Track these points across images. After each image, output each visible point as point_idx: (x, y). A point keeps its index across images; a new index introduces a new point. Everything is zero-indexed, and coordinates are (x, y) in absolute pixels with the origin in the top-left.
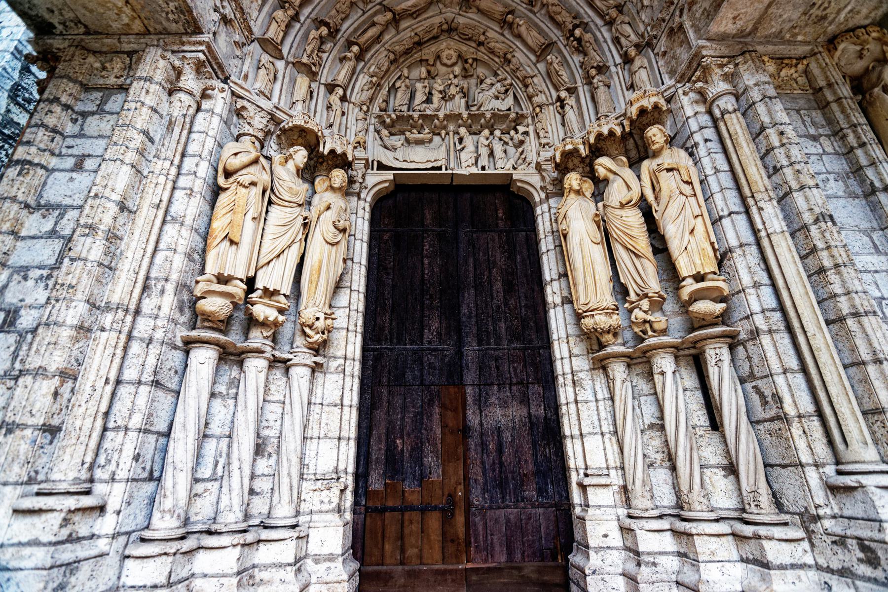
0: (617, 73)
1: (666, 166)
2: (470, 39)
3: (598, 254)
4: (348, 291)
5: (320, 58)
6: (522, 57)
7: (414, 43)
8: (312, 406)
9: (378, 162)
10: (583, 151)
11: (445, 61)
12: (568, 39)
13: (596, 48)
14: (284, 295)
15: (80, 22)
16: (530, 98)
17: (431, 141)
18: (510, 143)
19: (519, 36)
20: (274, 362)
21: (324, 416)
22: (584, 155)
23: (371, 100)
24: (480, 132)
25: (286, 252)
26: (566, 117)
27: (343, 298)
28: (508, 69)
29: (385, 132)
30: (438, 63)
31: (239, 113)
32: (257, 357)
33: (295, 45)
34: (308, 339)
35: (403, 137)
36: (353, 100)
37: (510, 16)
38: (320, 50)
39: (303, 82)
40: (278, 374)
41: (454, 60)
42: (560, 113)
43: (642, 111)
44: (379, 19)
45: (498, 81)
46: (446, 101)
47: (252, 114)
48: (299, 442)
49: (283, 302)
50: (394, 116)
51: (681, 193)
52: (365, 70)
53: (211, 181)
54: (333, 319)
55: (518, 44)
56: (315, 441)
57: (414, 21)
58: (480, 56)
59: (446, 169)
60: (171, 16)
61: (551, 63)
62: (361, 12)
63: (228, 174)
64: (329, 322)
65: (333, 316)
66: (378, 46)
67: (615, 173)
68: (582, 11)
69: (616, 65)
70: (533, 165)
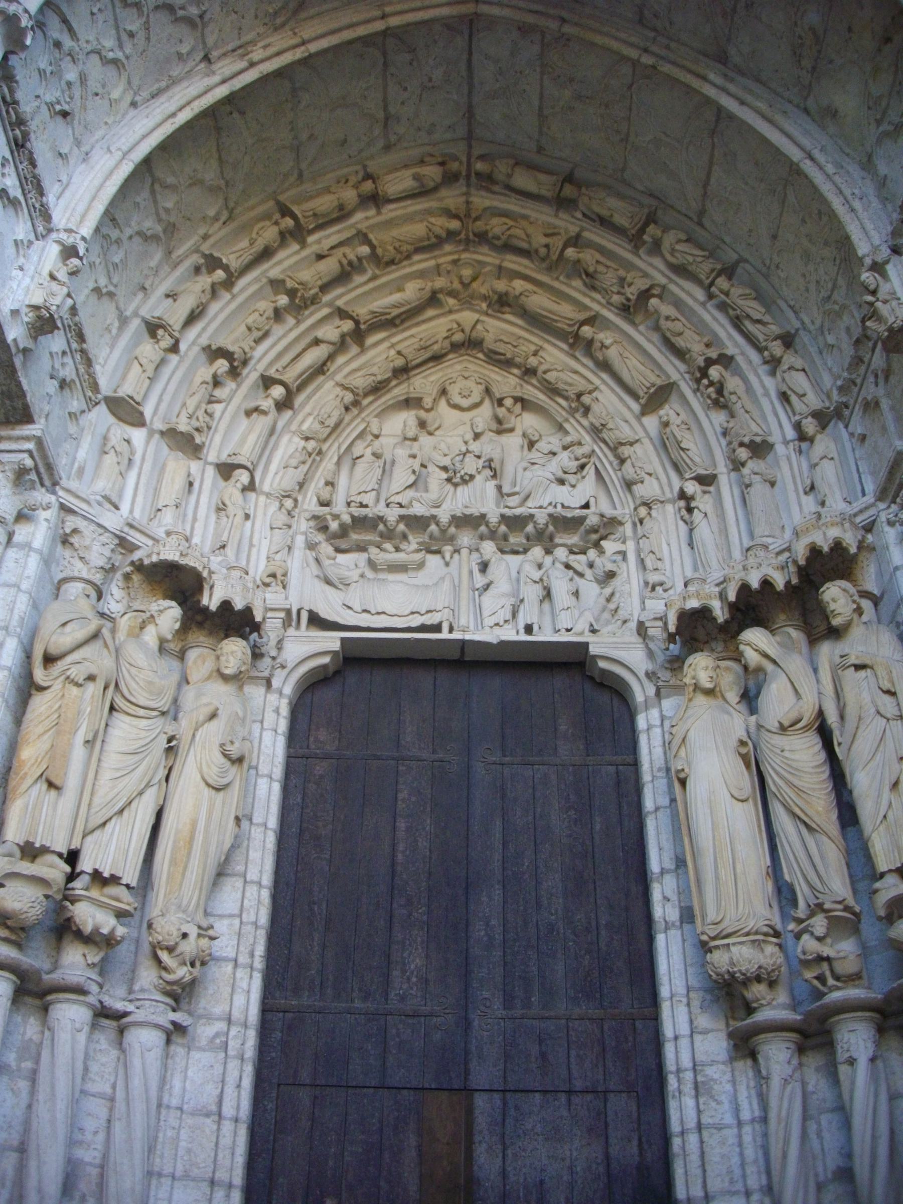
0: (789, 459)
1: (853, 660)
3: (743, 820)
4: (239, 883)
5: (211, 415)
6: (609, 402)
8: (164, 1112)
10: (720, 613)
11: (457, 400)
12: (698, 381)
14: (128, 886)
16: (629, 485)
17: (421, 565)
19: (605, 366)
20: (103, 1013)
21: (184, 1134)
22: (721, 620)
23: (301, 485)
24: (525, 551)
25: (134, 804)
27: (229, 897)
28: (585, 423)
29: (326, 549)
30: (443, 403)
31: (65, 541)
32: (75, 1002)
34: (164, 975)
35: (361, 558)
36: (266, 488)
40: (104, 1040)
41: (475, 398)
42: (685, 522)
43: (815, 552)
45: (565, 448)
46: (456, 485)
47: (87, 542)
48: (139, 1174)
49: (127, 900)
50: (346, 518)
51: (878, 712)
52: (294, 427)
53: (16, 671)
54: (212, 938)
56: (166, 1182)
59: (451, 630)
64: (204, 942)
65: (211, 933)
67: (774, 662)
69: (786, 443)
70: (633, 625)
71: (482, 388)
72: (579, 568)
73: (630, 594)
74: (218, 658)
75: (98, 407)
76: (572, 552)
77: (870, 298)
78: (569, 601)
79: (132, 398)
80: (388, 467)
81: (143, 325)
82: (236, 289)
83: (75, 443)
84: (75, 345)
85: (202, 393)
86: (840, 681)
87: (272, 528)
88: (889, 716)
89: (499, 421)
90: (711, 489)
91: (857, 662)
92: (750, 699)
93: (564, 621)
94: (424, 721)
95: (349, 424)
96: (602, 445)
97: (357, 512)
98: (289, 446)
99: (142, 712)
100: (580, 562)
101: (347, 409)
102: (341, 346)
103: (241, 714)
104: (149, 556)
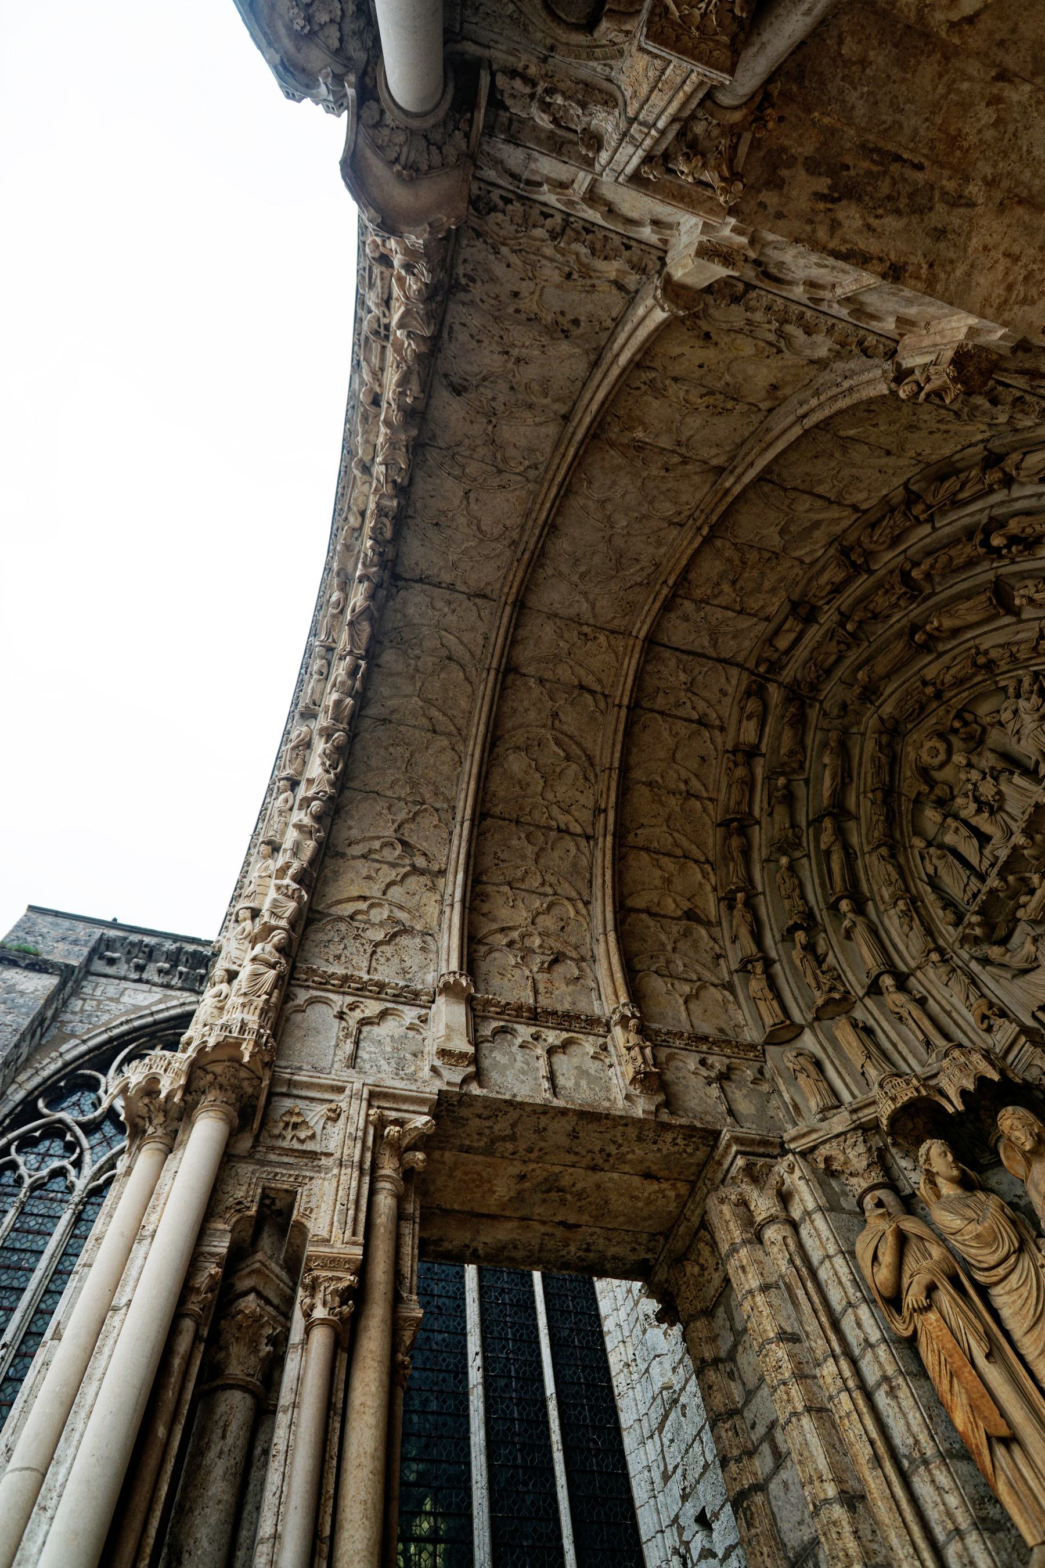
2: (922, 708)
7: (885, 802)
15: (654, 1235)
23: (929, 931)
33: (797, 993)
36: (913, 964)
38: (820, 960)
41: (942, 747)
44: (826, 838)
46: (1001, 808)
55: (969, 636)
60: (689, 1150)
62: (805, 861)
68: (967, 521)
82: (760, 889)
84: (704, 1048)
85: (810, 964)
95: (908, 861)
102: (840, 833)
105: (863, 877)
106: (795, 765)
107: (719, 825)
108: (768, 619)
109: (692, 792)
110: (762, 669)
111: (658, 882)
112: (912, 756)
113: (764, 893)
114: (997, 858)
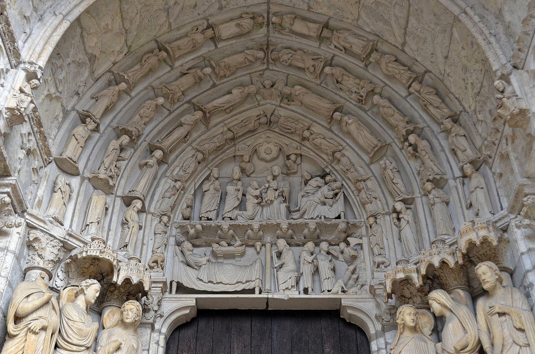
0: (456, 188)
1: (497, 310)
5: (119, 169)
9: (178, 283)
11: (263, 155)
13: (432, 157)
17: (243, 254)
18: (341, 257)
23: (173, 208)
24: (304, 244)
26: (403, 233)
29: (187, 245)
35: (209, 250)
36: (152, 210)
37: (337, 113)
39: (99, 200)
41: (274, 154)
42: (396, 225)
43: (471, 245)
44: (188, 119)
45: (326, 183)
46: (263, 207)
47: (43, 246)
50: (199, 227)
51: (514, 342)
52: (168, 174)
57: (227, 116)
58: (305, 151)
59: (260, 293)
61: (385, 169)
63: (18, 319)
66: (185, 145)
69: (455, 179)
70: (367, 287)
71: (277, 149)
72: (335, 254)
73: (365, 269)
74: (122, 313)
75: (51, 164)
76: (330, 245)
77: (500, 96)
78: (330, 274)
79: (71, 159)
80: (223, 196)
81: (78, 115)
82: (133, 94)
83: (36, 186)
85: (113, 156)
86: (490, 322)
87: (155, 234)
88: (521, 344)
89: (288, 168)
90: (412, 206)
91: (499, 311)
92: (437, 332)
93: (326, 285)
94: (245, 347)
95: (201, 172)
96: (348, 181)
97: (205, 223)
98: (165, 184)
99: (75, 348)
100: (335, 250)
101: (199, 163)
103: (135, 346)
104: (81, 253)
105: (177, 152)
106: (222, 73)
107: (157, 42)
108: (309, 8)
109: (170, 10)
110: (274, 19)
111: (103, 24)
112: (260, 141)
113: (132, 99)
114: (236, 218)
